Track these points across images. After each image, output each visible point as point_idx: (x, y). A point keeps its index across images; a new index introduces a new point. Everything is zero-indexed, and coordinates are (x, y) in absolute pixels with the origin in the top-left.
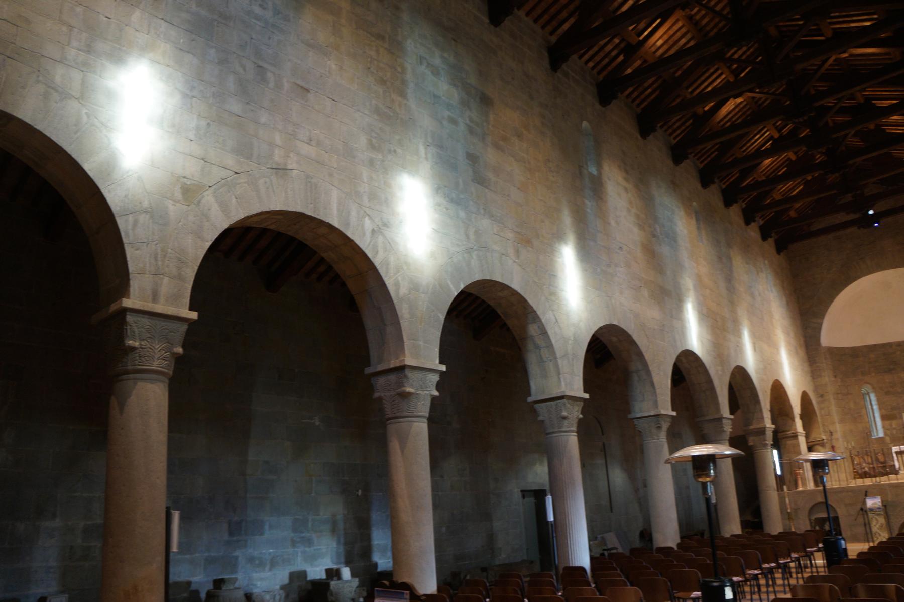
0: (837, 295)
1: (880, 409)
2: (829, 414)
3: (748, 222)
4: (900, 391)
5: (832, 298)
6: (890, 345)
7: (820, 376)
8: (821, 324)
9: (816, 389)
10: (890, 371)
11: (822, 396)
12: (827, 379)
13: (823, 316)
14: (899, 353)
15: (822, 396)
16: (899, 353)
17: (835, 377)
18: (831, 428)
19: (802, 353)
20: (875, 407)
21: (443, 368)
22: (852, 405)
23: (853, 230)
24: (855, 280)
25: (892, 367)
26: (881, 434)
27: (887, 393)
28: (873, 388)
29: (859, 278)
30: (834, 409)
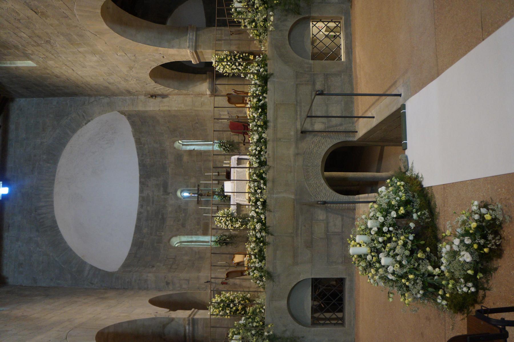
0: (66, 243)
1: (197, 235)
2: (188, 280)
4: (183, 215)
5: (67, 249)
6: (139, 213)
7: (146, 281)
8: (92, 267)
10: (163, 220)
11: (168, 284)
12: (149, 275)
13: (84, 263)
14: (149, 208)
15: (168, 284)
16: (149, 208)
17: (153, 267)
18: (203, 280)
20: (194, 238)
22: (186, 258)
24: (55, 222)
25: (160, 216)
27: (183, 225)
28: (176, 236)
29: (54, 217)
30: (183, 275)
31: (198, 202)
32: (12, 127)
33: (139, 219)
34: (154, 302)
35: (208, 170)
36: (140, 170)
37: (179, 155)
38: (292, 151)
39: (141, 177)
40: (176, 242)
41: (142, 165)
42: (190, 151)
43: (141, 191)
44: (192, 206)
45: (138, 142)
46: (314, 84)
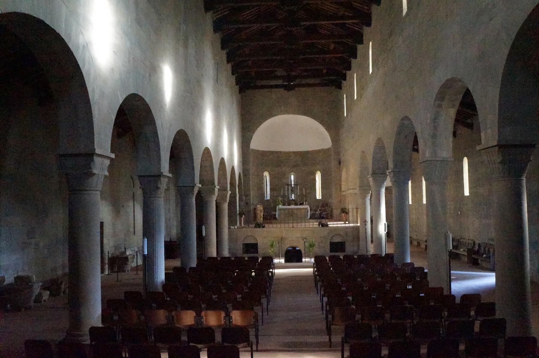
3: (233, 74)
6: (281, 152)
9: (243, 171)
13: (254, 133)
19: (241, 149)
20: (268, 184)
21: (113, 156)
23: (282, 90)
26: (268, 198)
31: (288, 185)
32: (322, 88)
33: (277, 152)
34: (240, 174)
35: (306, 190)
36: (304, 152)
37: (314, 174)
38: (298, 236)
39: (301, 152)
40: (266, 174)
41: (307, 153)
42: (315, 180)
43: (294, 152)
44: (285, 181)
45: (319, 151)
46: (321, 243)
